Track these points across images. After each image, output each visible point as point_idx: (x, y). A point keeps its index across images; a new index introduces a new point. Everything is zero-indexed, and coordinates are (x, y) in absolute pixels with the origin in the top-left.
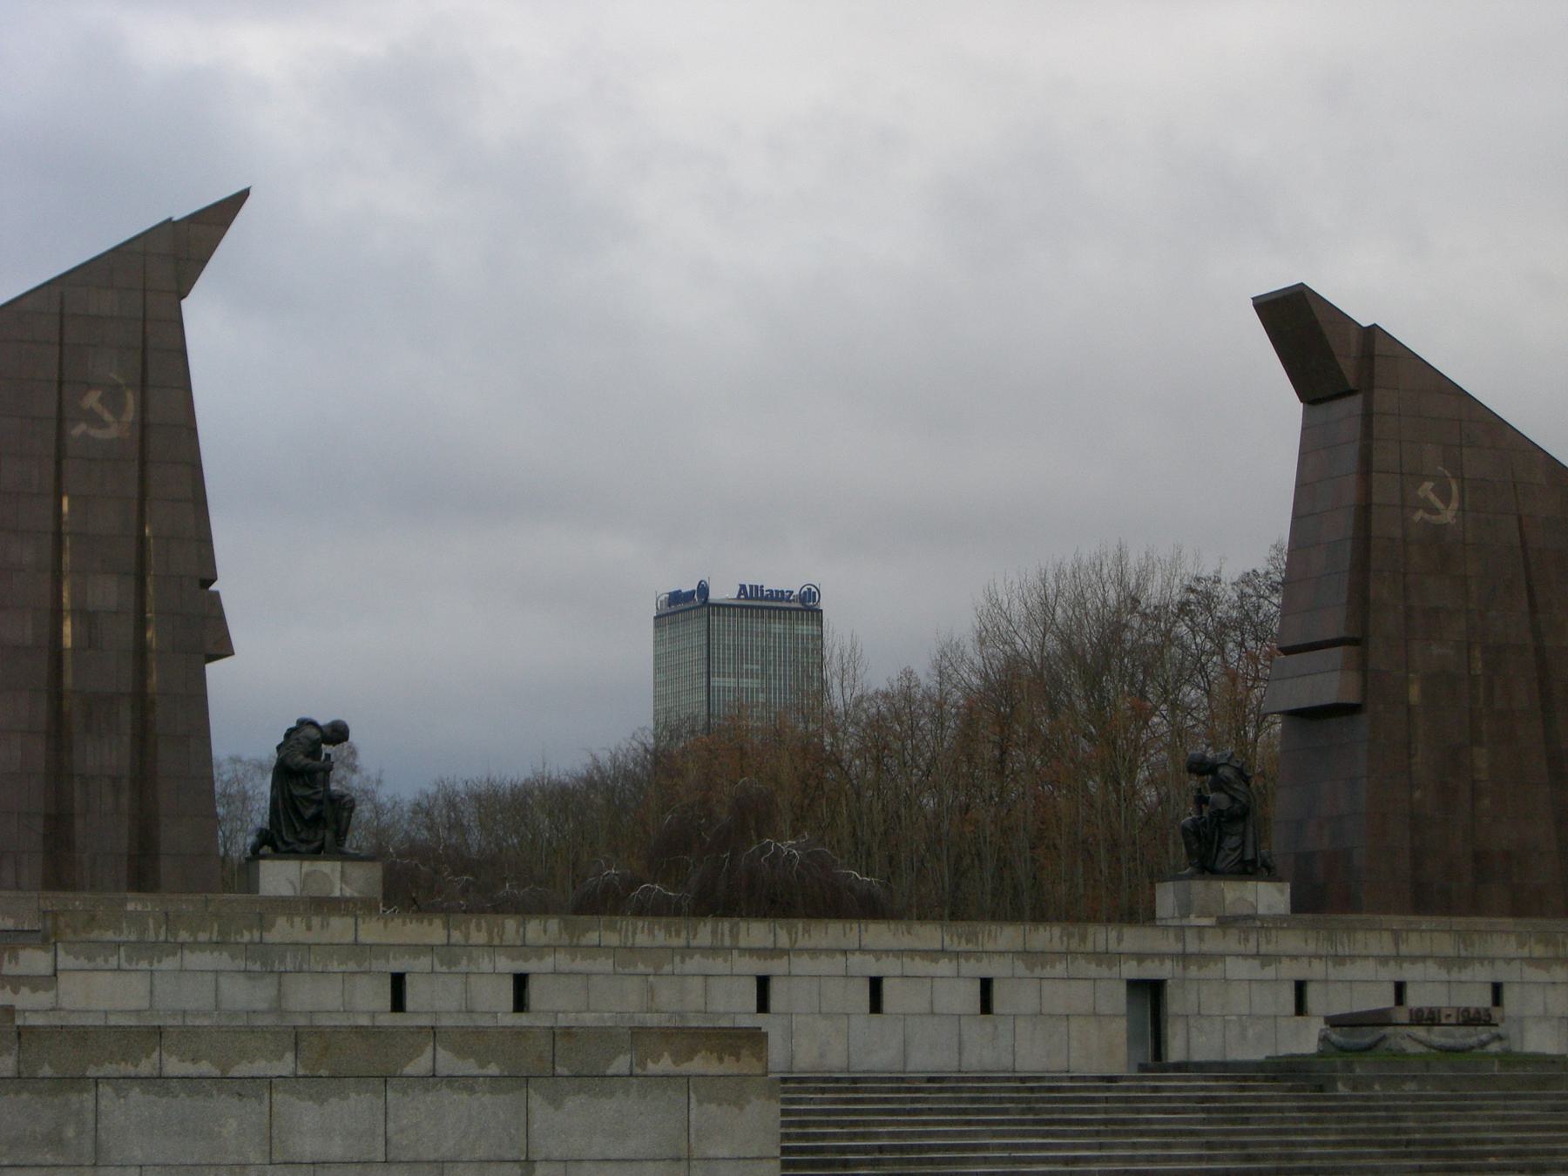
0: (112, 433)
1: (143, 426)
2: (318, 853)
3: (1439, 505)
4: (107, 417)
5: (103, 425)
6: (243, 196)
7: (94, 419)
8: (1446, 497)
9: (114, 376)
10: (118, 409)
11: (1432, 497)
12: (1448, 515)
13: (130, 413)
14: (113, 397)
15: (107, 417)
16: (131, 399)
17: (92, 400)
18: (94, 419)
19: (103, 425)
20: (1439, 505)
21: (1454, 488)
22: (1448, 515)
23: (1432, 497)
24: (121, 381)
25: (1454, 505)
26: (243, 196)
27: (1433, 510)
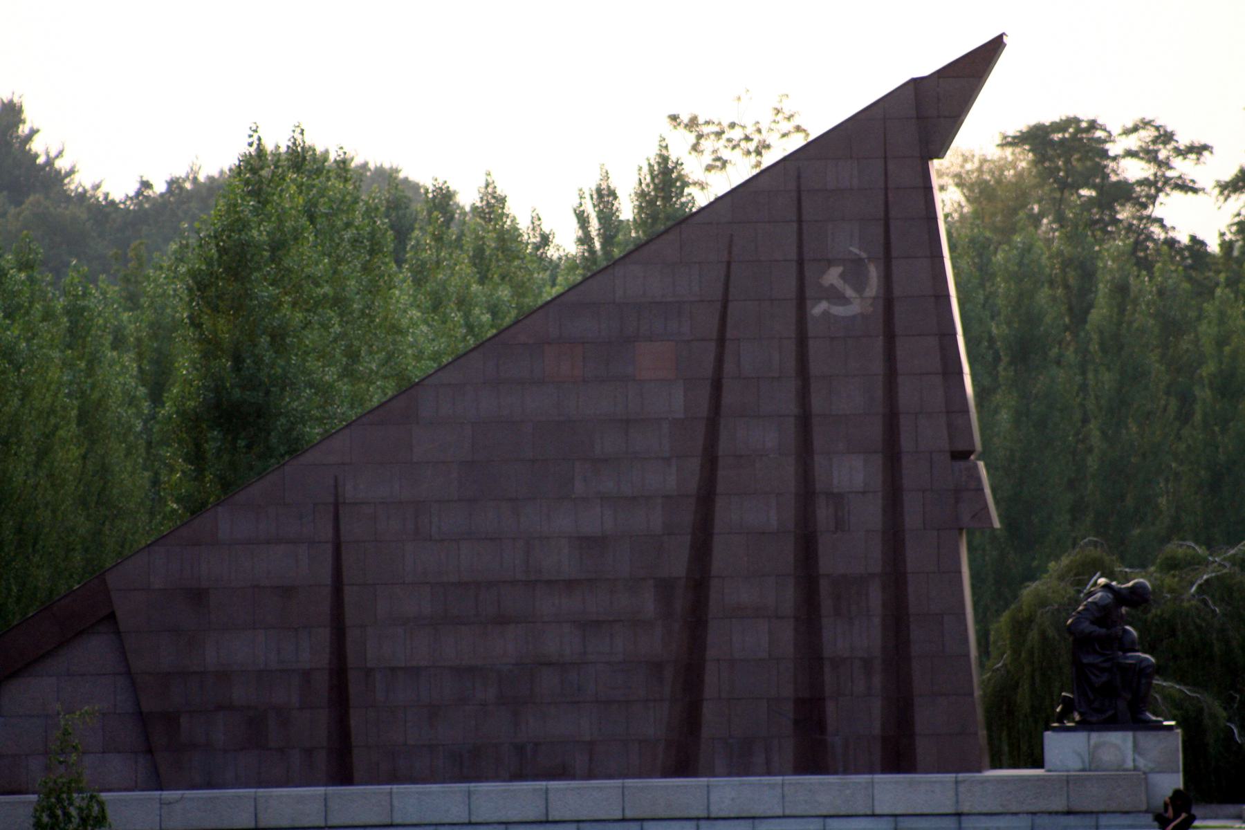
0: (855, 308)
1: (888, 302)
2: (1111, 723)
4: (849, 292)
5: (844, 300)
6: (994, 48)
7: (836, 297)
9: (856, 251)
10: (860, 287)
15: (849, 292)
16: (874, 273)
17: (833, 276)
18: (836, 297)
19: (844, 300)
24: (864, 255)
26: (994, 48)
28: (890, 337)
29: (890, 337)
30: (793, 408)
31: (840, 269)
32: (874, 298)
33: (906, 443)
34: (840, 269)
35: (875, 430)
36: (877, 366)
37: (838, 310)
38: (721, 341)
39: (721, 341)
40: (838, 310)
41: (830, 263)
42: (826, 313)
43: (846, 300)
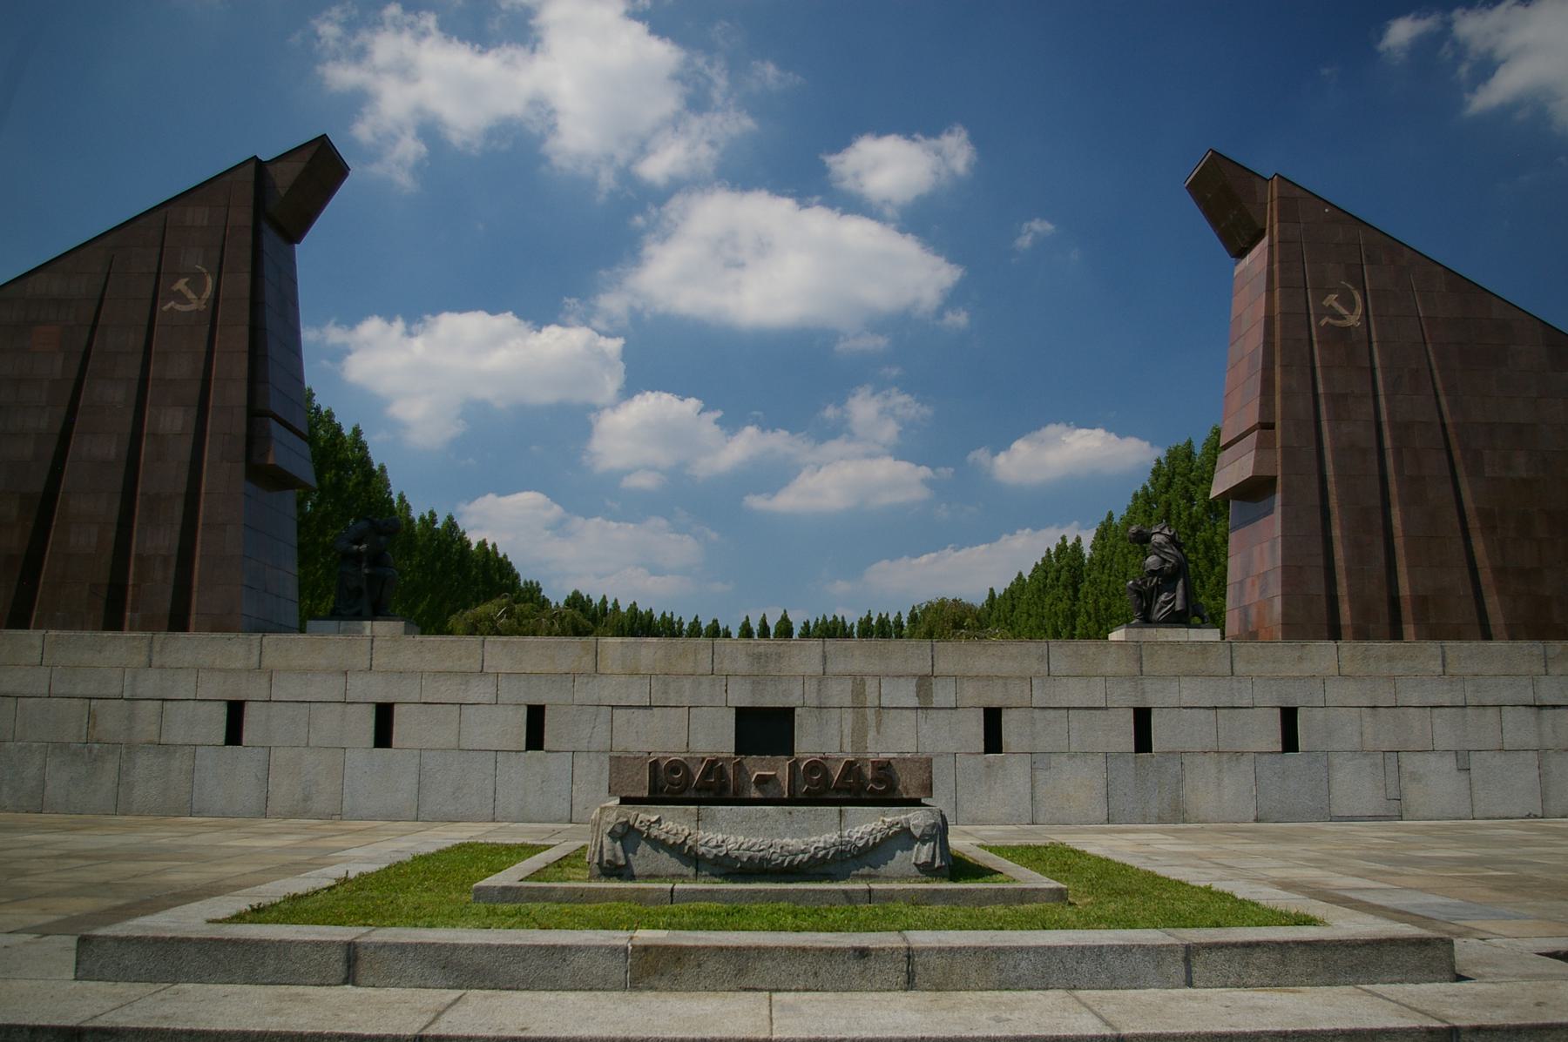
0: (193, 307)
3: (1343, 311)
4: (191, 296)
5: (188, 302)
8: (1350, 305)
10: (198, 293)
11: (1336, 305)
12: (1353, 320)
13: (208, 292)
14: (196, 283)
15: (191, 296)
17: (181, 285)
19: (188, 302)
20: (1343, 311)
21: (1358, 297)
22: (1353, 320)
23: (1336, 305)
25: (1359, 310)
27: (1342, 317)
36: (203, 348)
37: (184, 308)
38: (94, 327)
39: (94, 327)
40: (178, 307)
41: (179, 276)
43: (188, 299)
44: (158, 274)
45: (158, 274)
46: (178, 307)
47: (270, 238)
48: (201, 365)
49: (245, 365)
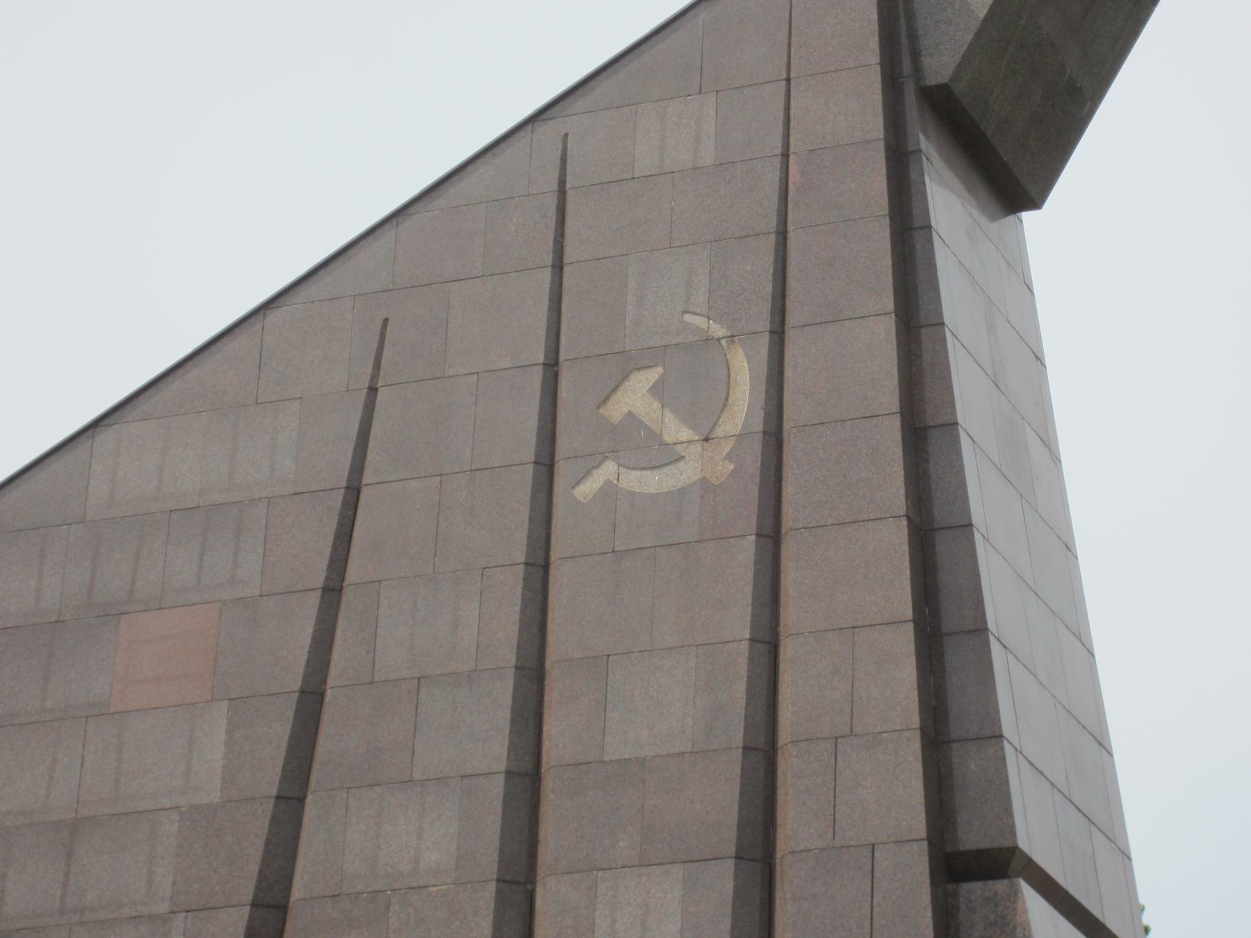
0: (687, 473)
4: (675, 430)
5: (668, 456)
15: (675, 430)
16: (744, 374)
17: (636, 396)
19: (668, 456)
24: (718, 331)
28: (771, 537)
29: (771, 537)
30: (493, 752)
31: (655, 374)
32: (741, 437)
33: (797, 827)
34: (655, 374)
35: (718, 799)
36: (738, 624)
38: (333, 591)
39: (333, 591)
40: (632, 480)
41: (628, 364)
42: (609, 491)
43: (663, 451)
44: (552, 368)
45: (552, 368)
46: (632, 480)
47: (948, 203)
48: (737, 691)
49: (907, 673)
